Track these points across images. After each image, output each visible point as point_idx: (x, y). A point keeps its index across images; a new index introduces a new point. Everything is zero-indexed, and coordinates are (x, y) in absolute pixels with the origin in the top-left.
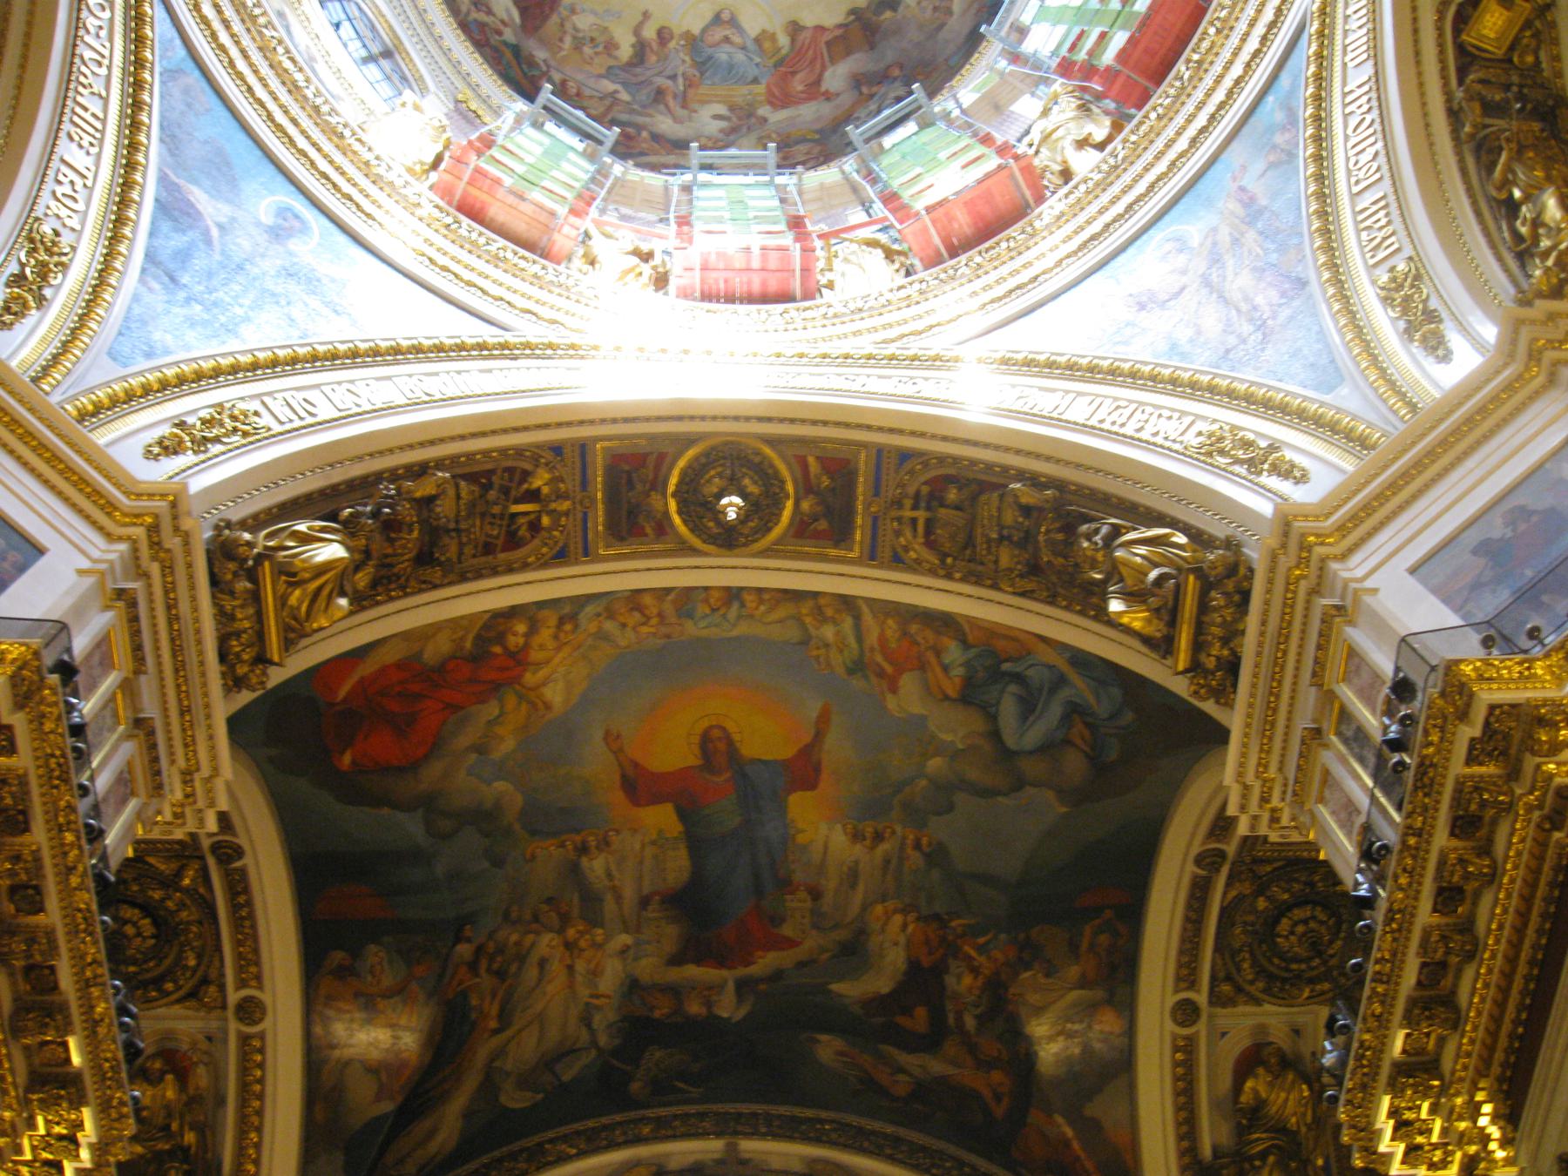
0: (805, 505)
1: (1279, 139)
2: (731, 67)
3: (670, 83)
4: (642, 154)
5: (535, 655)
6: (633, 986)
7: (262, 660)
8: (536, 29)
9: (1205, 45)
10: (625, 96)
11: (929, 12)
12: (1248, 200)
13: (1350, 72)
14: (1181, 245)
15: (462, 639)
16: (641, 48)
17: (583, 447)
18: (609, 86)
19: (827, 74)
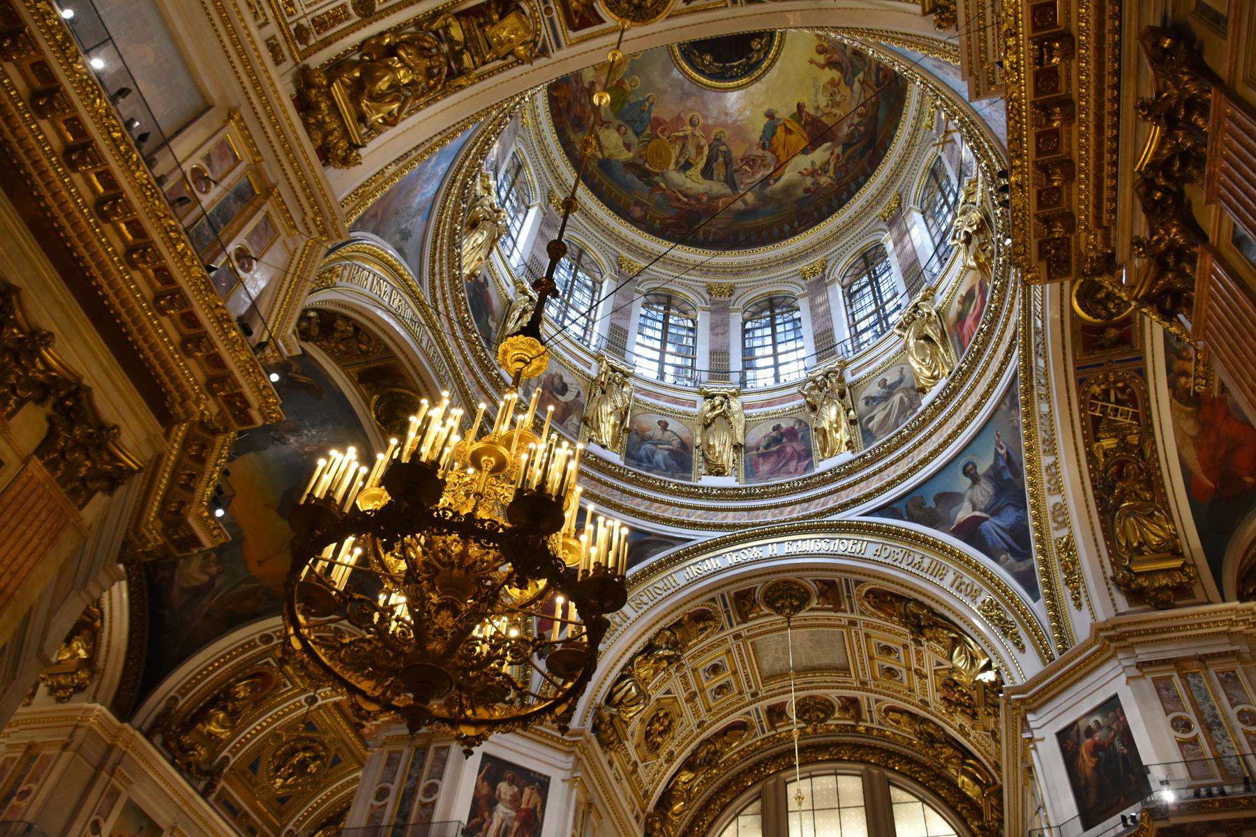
7: (1181, 569)
10: (861, 75)
15: (1187, 413)
16: (831, 64)
17: (1078, 369)
18: (856, 85)
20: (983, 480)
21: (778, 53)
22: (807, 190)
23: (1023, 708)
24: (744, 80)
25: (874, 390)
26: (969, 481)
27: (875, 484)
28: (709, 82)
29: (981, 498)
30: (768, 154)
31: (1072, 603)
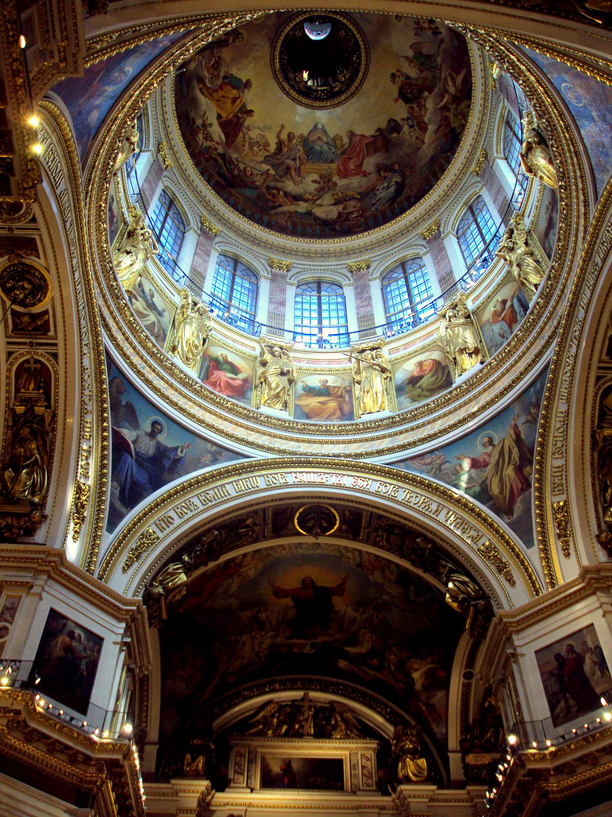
0: (344, 527)
1: (532, 411)
2: (321, 153)
3: (293, 162)
4: (280, 206)
5: (244, 563)
6: (273, 646)
8: (233, 142)
9: (513, 343)
10: (272, 172)
11: (414, 138)
12: (518, 435)
13: (560, 405)
14: (491, 442)
16: (280, 144)
17: (264, 510)
18: (265, 167)
19: (365, 161)
20: (154, 442)
21: (293, 99)
22: (194, 121)
23: (49, 568)
24: (278, 65)
25: (147, 287)
26: (149, 430)
27: (120, 337)
28: (284, 34)
29: (142, 445)
30: (219, 82)
31: (123, 564)
